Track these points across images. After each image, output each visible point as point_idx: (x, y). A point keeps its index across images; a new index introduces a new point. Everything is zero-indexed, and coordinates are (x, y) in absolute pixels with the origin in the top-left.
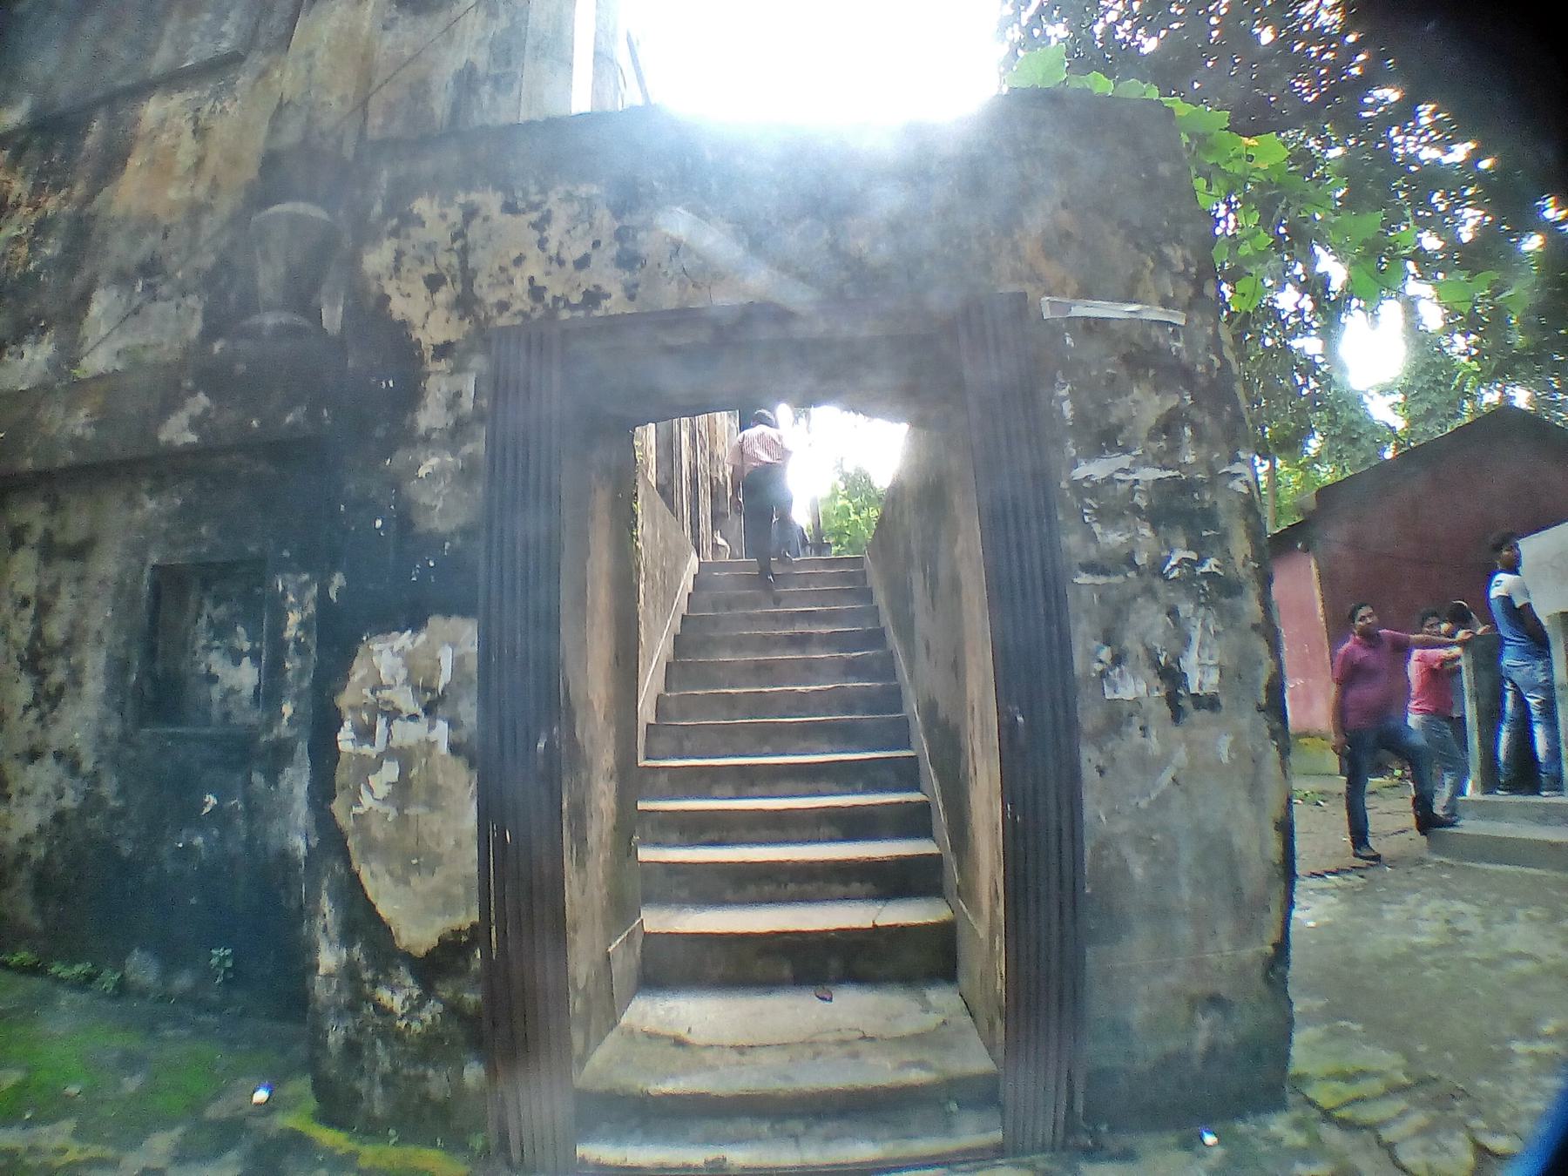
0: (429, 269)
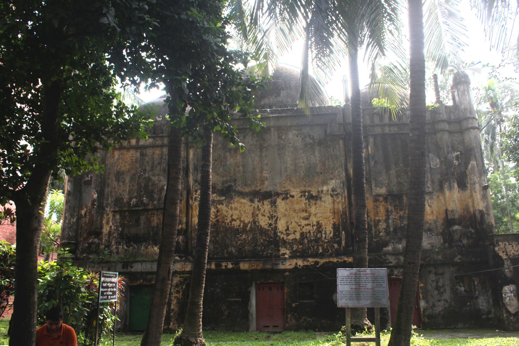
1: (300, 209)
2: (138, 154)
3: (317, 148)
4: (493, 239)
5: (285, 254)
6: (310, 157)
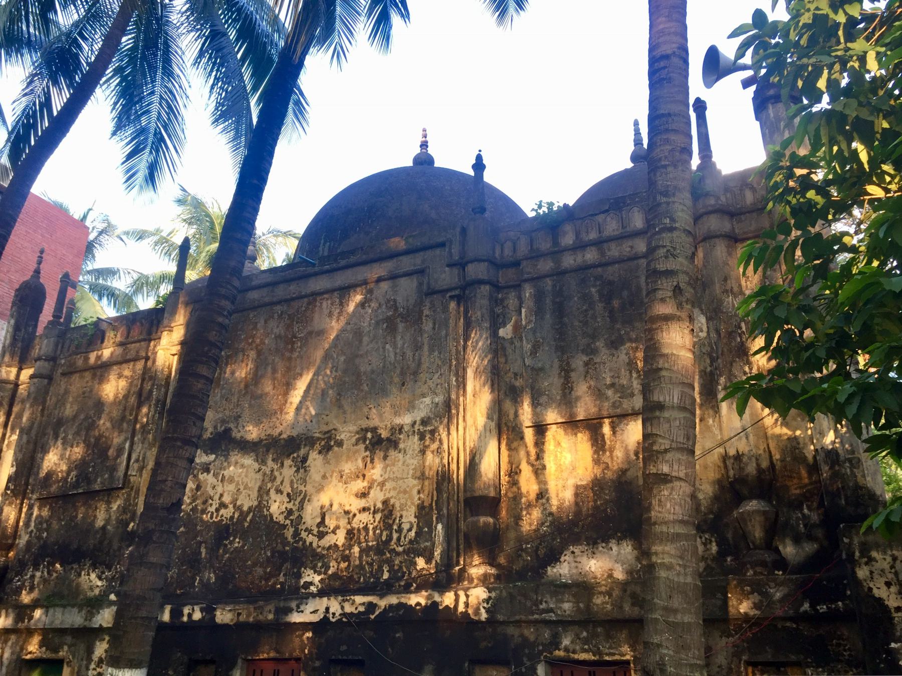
0: (885, 579)
1: (351, 473)
3: (401, 326)
5: (311, 583)
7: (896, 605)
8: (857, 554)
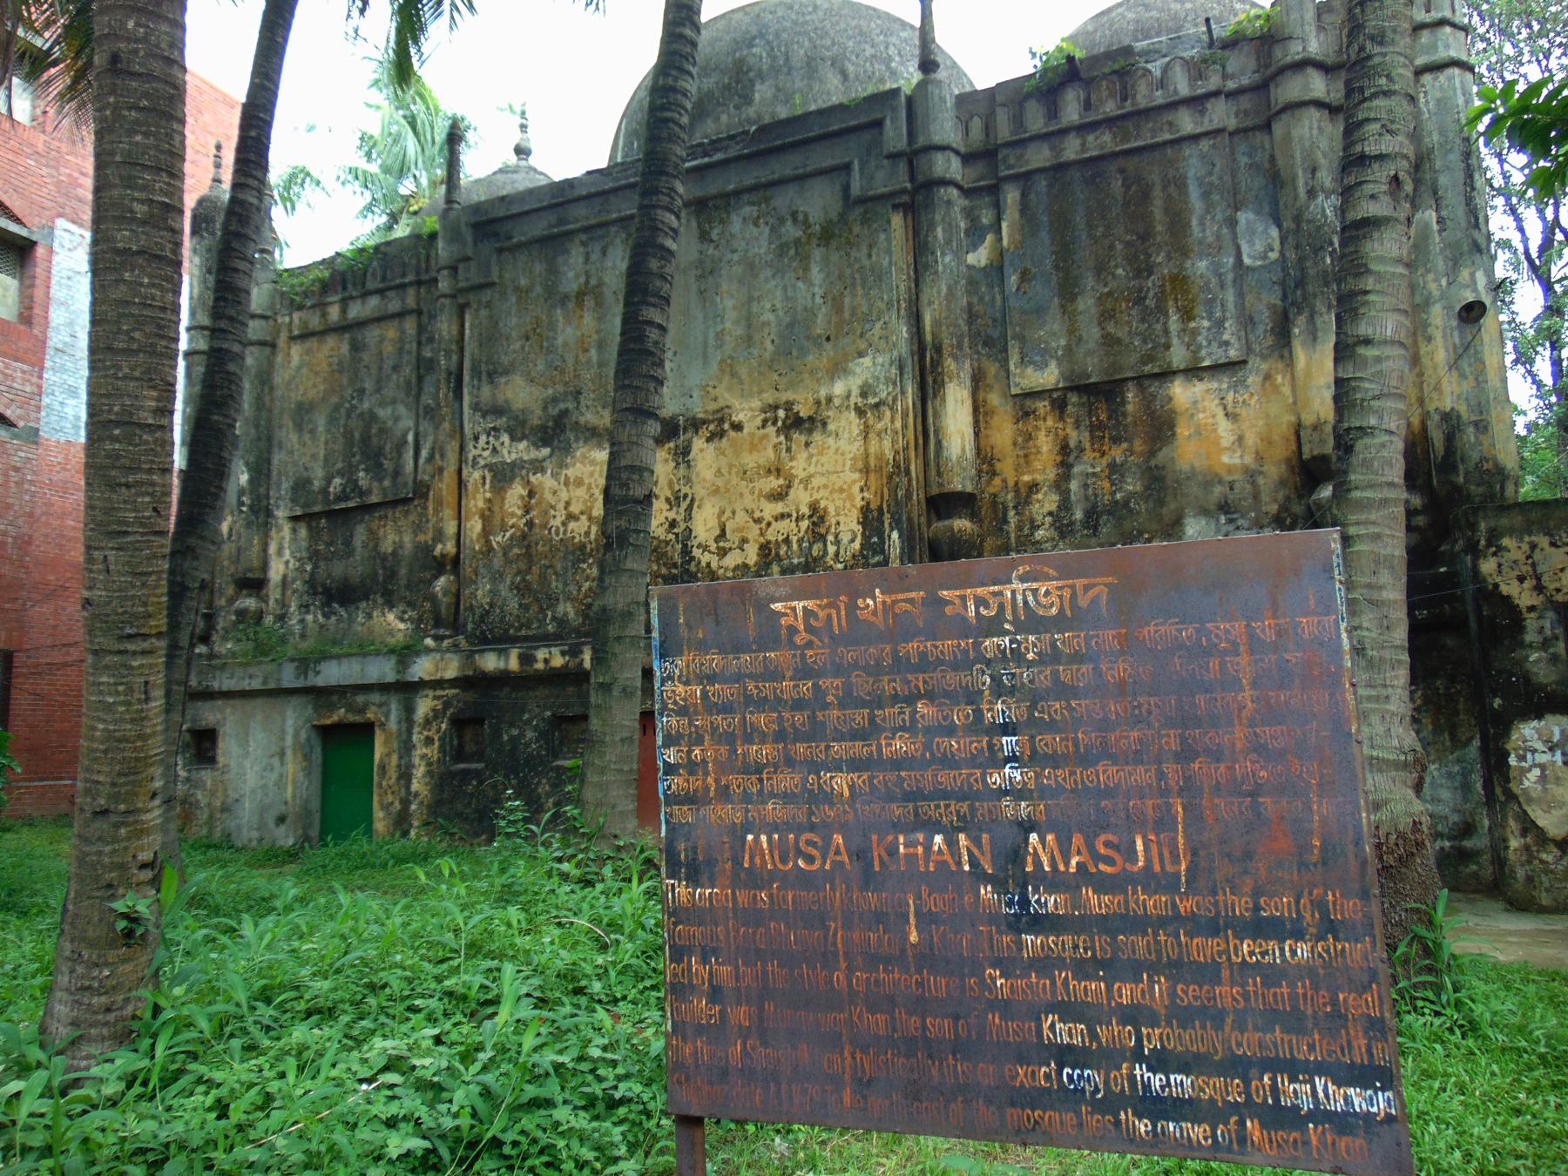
0: (1517, 573)
1: (759, 467)
2: (345, 348)
4: (1473, 526)
6: (794, 287)
7: (1529, 603)
8: (1483, 542)
